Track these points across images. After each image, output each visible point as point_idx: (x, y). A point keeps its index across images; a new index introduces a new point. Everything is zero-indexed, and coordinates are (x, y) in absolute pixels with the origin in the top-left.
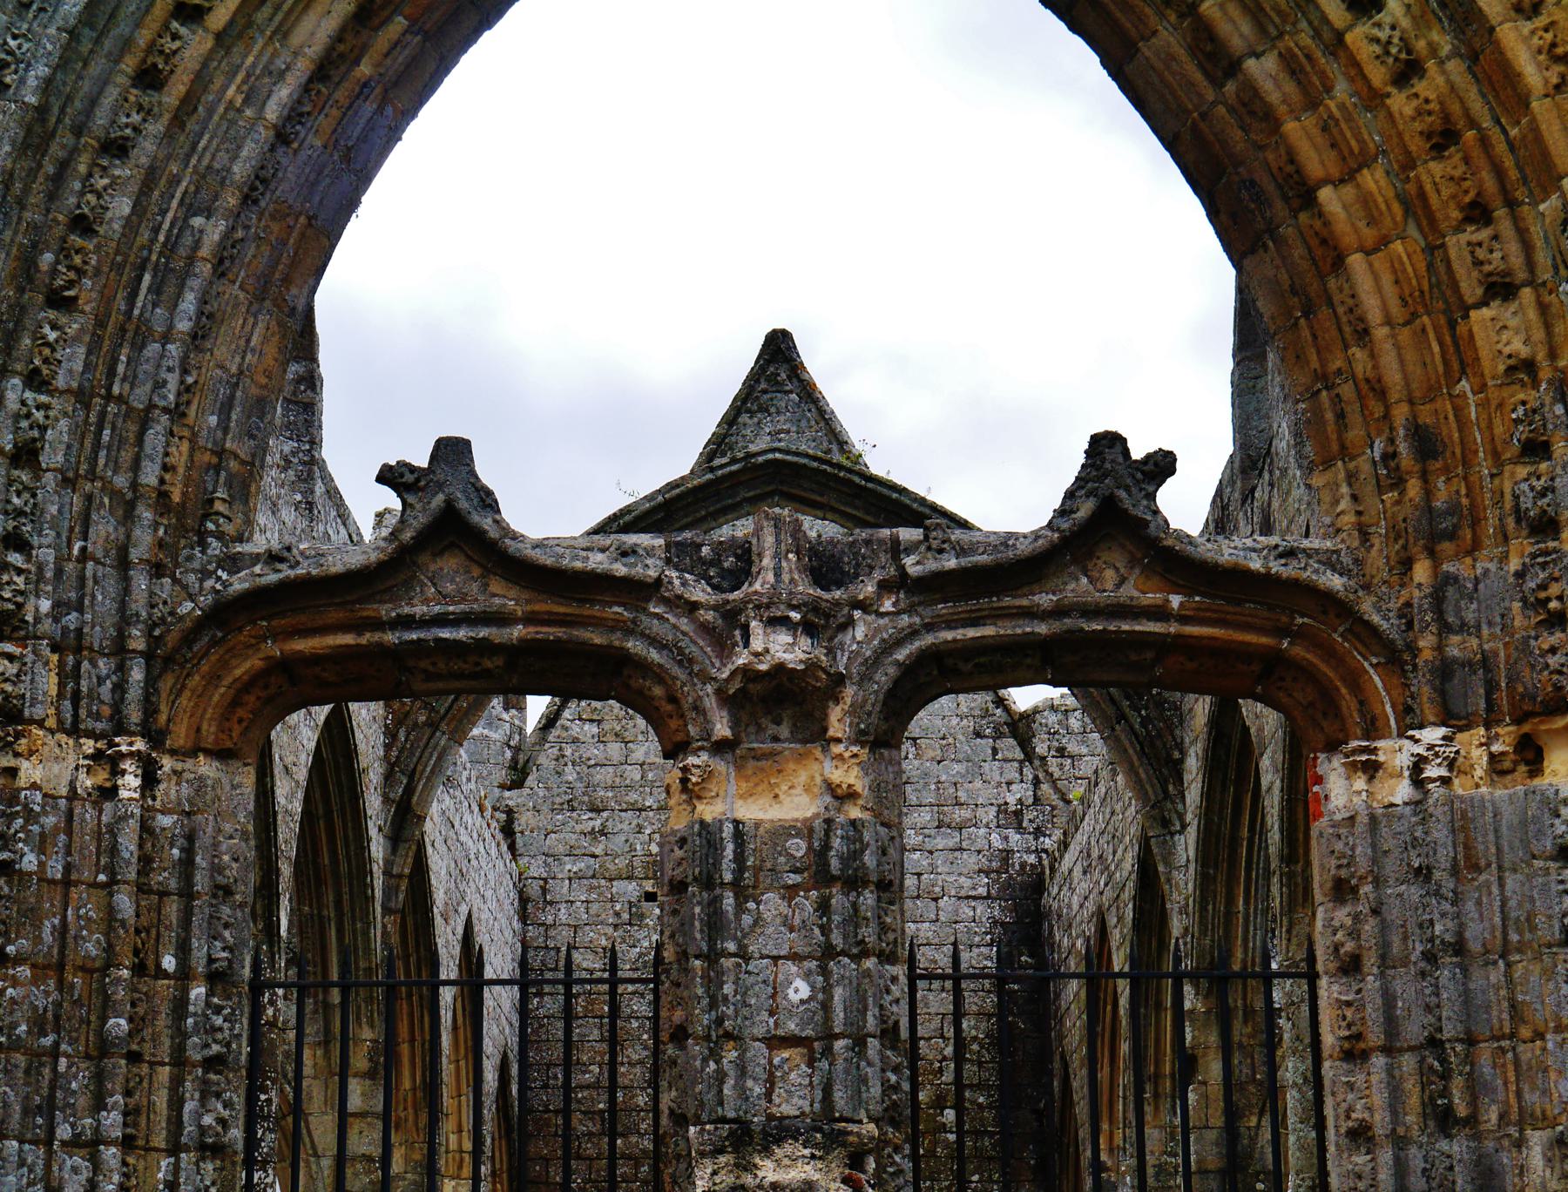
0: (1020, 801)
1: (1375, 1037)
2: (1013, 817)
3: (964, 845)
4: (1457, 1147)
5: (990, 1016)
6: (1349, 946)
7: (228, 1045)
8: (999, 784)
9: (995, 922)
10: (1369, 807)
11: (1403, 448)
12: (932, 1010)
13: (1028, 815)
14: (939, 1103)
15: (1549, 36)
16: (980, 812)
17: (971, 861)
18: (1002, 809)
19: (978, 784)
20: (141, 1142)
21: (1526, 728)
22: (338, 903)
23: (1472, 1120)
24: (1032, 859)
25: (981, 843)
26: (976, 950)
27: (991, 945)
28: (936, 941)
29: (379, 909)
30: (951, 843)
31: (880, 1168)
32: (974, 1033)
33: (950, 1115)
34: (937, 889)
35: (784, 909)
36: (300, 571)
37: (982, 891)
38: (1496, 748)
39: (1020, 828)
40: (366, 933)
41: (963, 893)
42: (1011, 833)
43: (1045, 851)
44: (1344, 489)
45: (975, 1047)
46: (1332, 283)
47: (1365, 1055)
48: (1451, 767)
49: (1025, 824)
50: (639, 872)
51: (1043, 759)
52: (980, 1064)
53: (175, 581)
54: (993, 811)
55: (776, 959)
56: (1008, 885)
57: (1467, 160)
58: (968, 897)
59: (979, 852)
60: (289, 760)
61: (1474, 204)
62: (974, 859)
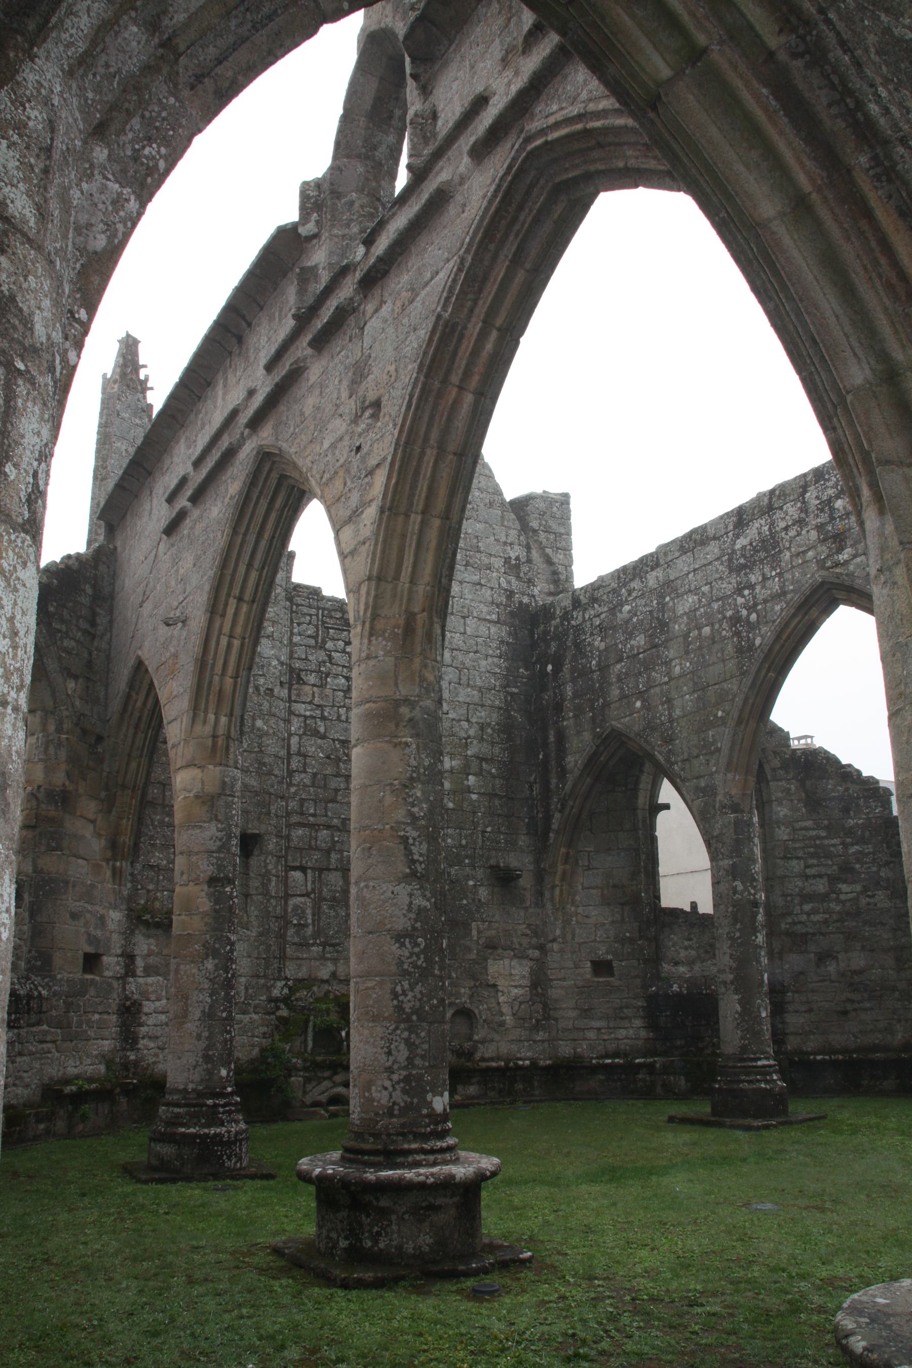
0: (517, 558)
2: (513, 567)
3: (483, 582)
5: (500, 708)
8: (505, 543)
9: (502, 642)
12: (461, 699)
13: (524, 568)
16: (493, 559)
18: (507, 560)
24: (526, 600)
26: (490, 660)
27: (500, 657)
28: (465, 648)
30: (476, 578)
32: (488, 720)
34: (465, 610)
37: (494, 617)
39: (518, 577)
41: (483, 616)
42: (513, 580)
43: (534, 596)
45: (489, 731)
49: (522, 575)
51: (535, 531)
52: (493, 744)
56: (512, 614)
58: (485, 620)
59: (492, 589)
62: (489, 592)
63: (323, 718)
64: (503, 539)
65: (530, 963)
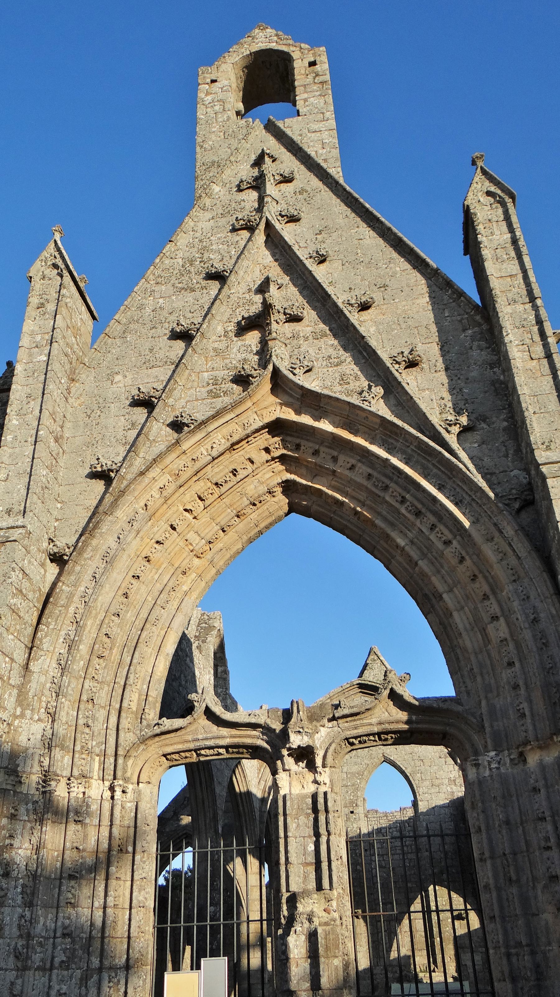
1: (487, 854)
4: (514, 890)
6: (477, 823)
7: (148, 873)
10: (478, 778)
11: (474, 667)
14: (442, 873)
15: (496, 547)
16: (443, 781)
17: (442, 796)
18: (449, 779)
19: (442, 772)
20: (120, 907)
21: (520, 750)
22: (246, 821)
23: (518, 881)
25: (445, 790)
29: (258, 822)
31: (338, 905)
33: (445, 876)
35: (306, 821)
36: (166, 728)
38: (512, 757)
40: (254, 829)
42: (454, 788)
44: (461, 680)
46: (450, 620)
47: (485, 860)
48: (499, 763)
50: (348, 805)
53: (134, 733)
54: (447, 780)
55: (304, 837)
57: (480, 583)
60: (220, 780)
61: (485, 595)
63: (384, 860)
64: (447, 769)
65: (480, 955)
